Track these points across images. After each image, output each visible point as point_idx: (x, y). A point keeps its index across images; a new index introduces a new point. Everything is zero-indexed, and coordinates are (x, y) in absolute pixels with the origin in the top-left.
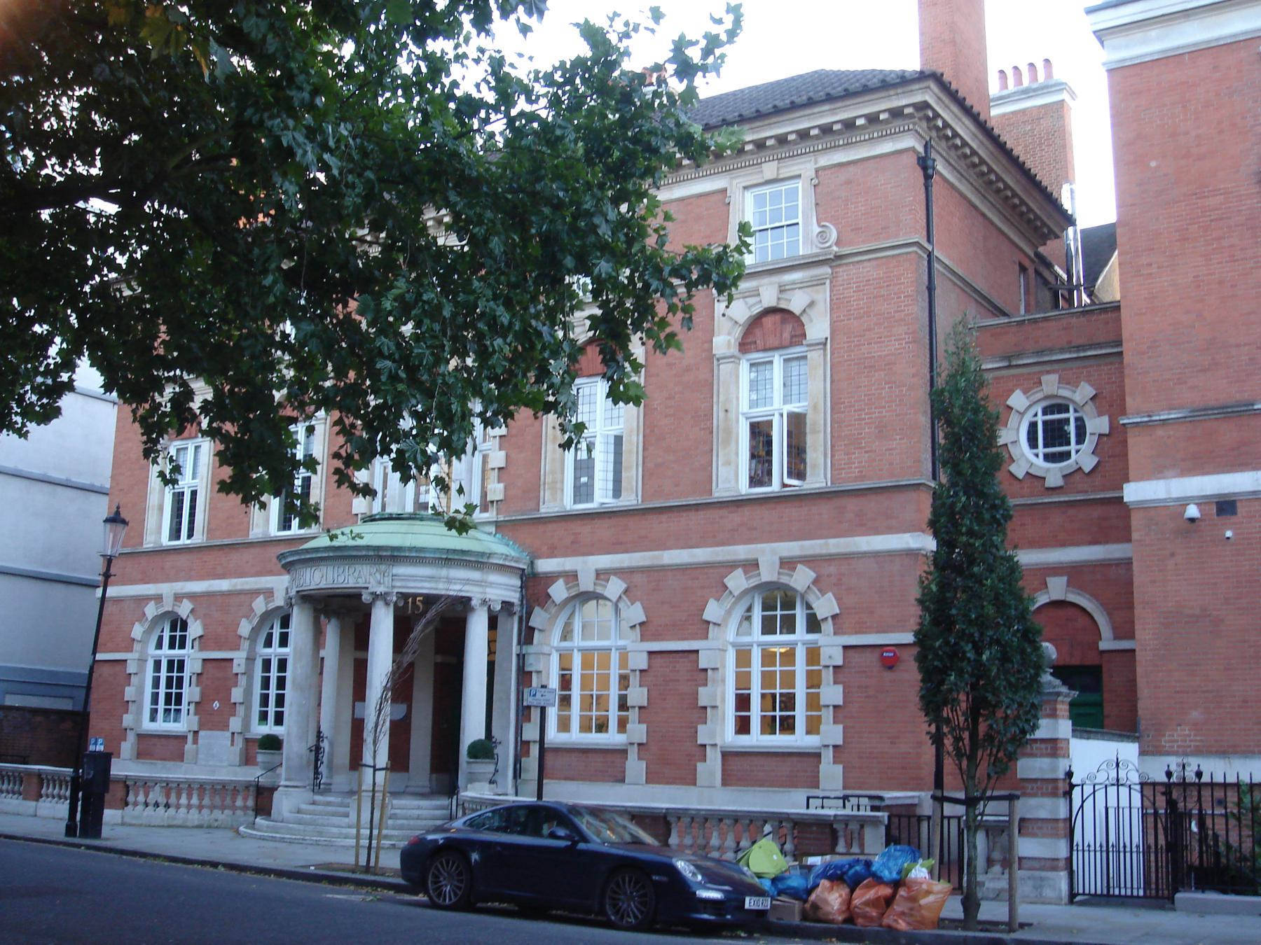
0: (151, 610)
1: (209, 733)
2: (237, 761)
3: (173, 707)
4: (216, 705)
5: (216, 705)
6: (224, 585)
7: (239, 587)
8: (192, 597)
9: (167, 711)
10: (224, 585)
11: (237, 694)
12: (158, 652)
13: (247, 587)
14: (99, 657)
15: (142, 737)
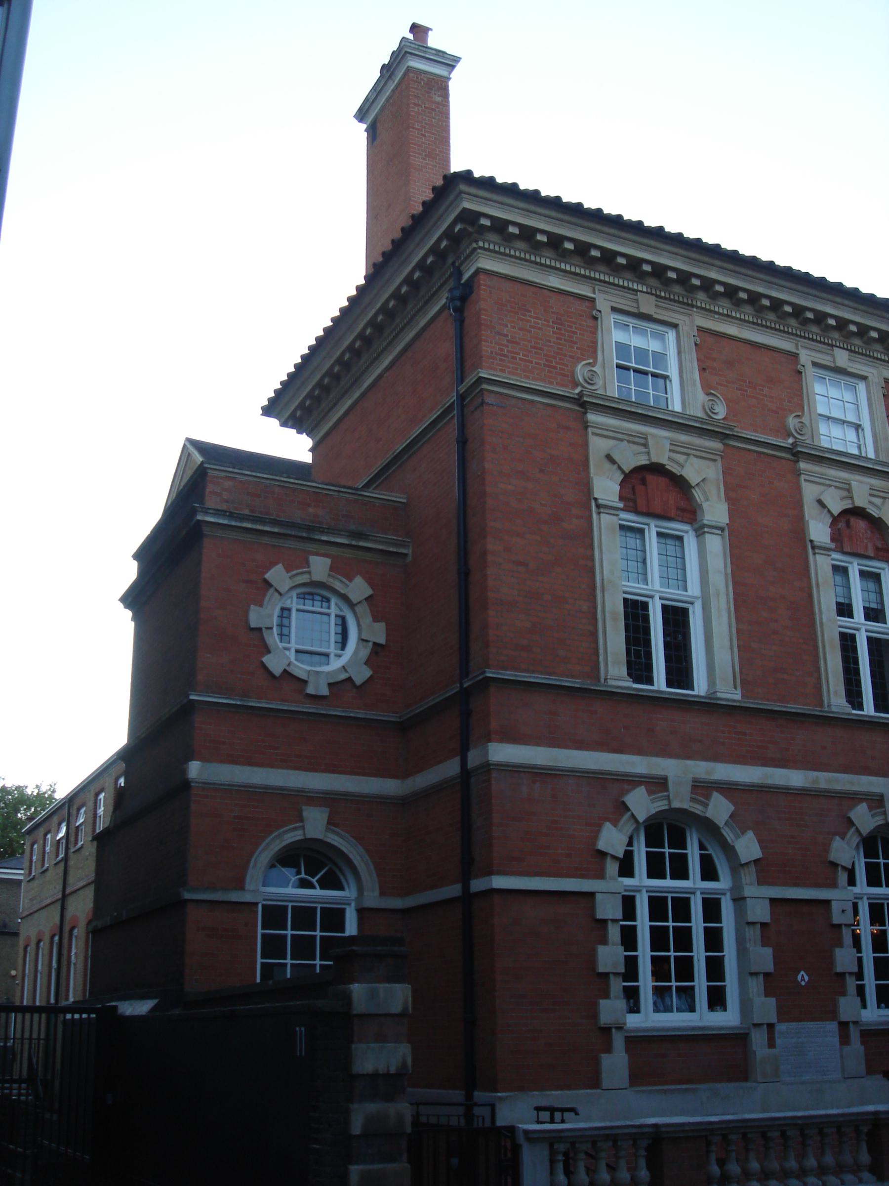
0: (642, 805)
1: (793, 1025)
2: (862, 1068)
3: (674, 984)
4: (803, 977)
5: (803, 977)
6: (796, 778)
7: (823, 785)
8: (728, 789)
9: (660, 993)
10: (796, 778)
11: (844, 959)
12: (627, 881)
13: (838, 787)
14: (477, 885)
15: (638, 1043)
